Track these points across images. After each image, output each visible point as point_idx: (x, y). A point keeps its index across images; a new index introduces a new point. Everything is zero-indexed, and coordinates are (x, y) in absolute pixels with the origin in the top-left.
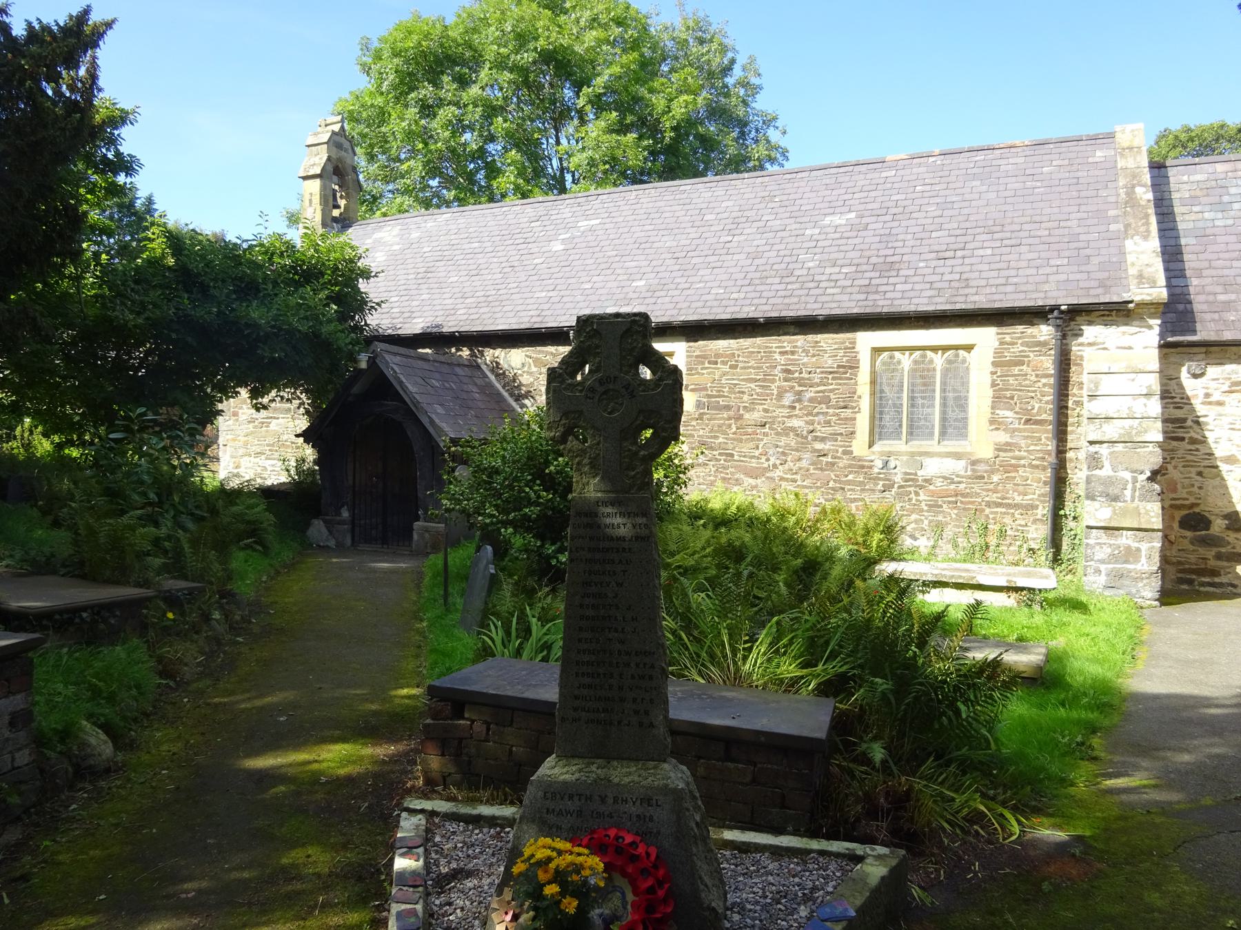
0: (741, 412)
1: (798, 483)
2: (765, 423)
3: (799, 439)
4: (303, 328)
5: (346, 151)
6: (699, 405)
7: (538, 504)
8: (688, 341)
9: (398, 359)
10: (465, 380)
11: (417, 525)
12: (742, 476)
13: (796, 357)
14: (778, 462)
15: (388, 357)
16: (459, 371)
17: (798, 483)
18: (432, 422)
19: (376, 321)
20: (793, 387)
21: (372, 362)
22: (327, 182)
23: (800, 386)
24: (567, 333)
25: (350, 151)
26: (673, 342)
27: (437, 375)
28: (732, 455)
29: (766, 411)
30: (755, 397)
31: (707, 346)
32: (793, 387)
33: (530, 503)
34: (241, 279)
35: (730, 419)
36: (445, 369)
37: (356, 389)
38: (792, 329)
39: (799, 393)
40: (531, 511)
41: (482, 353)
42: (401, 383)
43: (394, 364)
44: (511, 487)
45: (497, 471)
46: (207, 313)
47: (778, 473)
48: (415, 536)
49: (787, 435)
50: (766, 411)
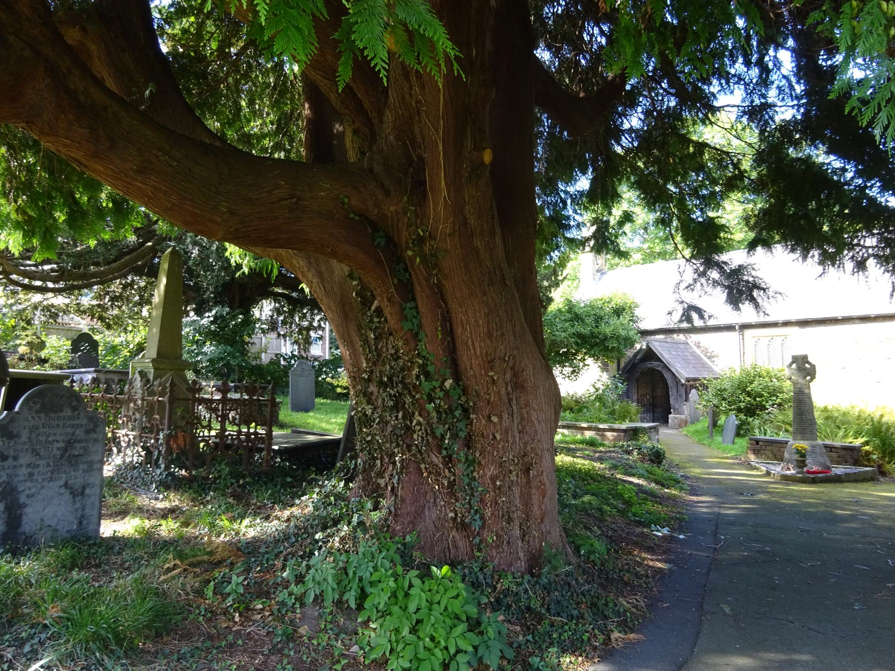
4: (623, 333)
7: (744, 402)
9: (657, 343)
10: (684, 350)
11: (670, 416)
15: (654, 343)
16: (680, 346)
18: (677, 371)
19: (646, 325)
21: (648, 345)
24: (735, 327)
27: (673, 349)
33: (740, 402)
34: (595, 315)
36: (675, 346)
37: (638, 357)
38: (857, 321)
40: (742, 405)
41: (690, 337)
42: (661, 354)
43: (658, 344)
44: (732, 396)
45: (725, 389)
46: (586, 331)
48: (670, 421)
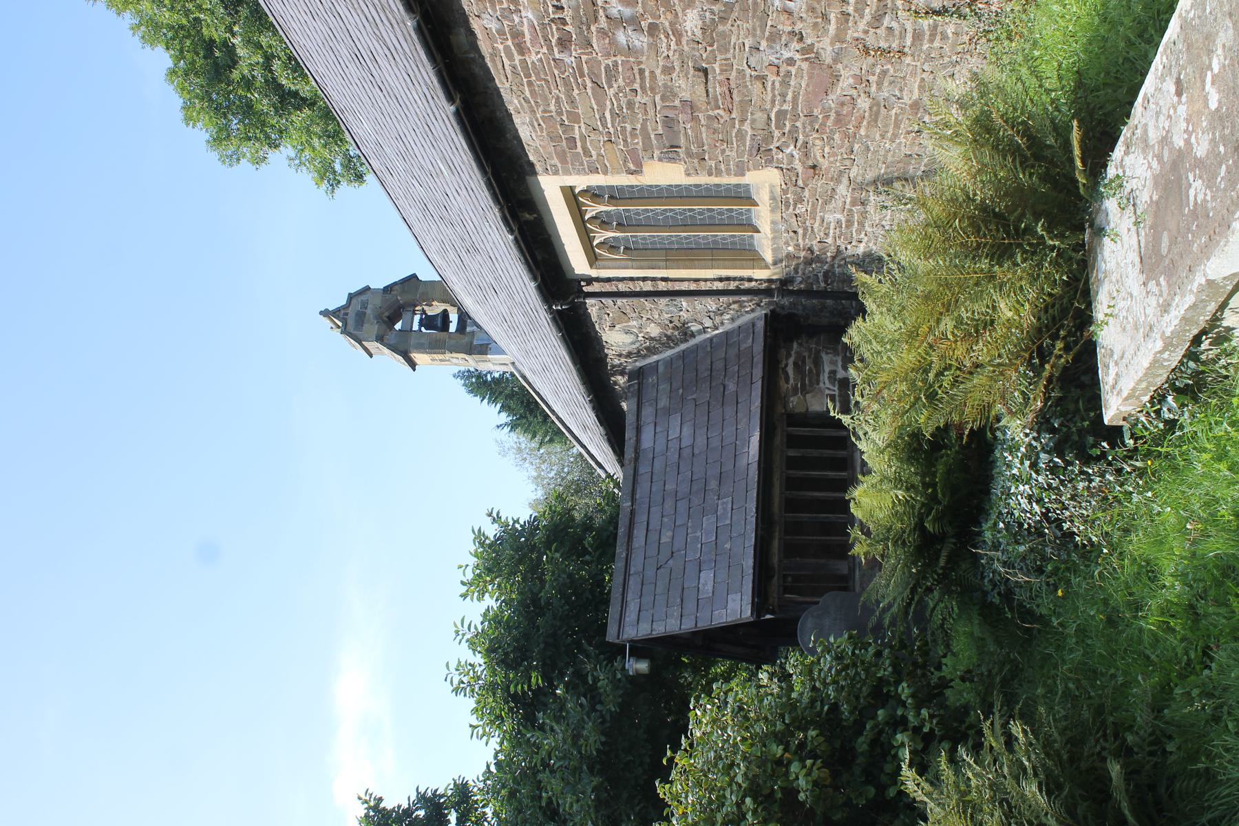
0: (677, 103)
1: (851, 9)
2: (697, 69)
3: (734, 15)
5: (364, 305)
6: (671, 152)
8: (535, 173)
12: (832, 96)
13: (526, 29)
14: (795, 45)
17: (851, 9)
20: (601, 31)
22: (413, 340)
23: (596, 19)
25: (363, 298)
26: (542, 191)
28: (781, 115)
29: (668, 70)
30: (637, 86)
31: (536, 150)
32: (601, 31)
35: (695, 119)
38: (460, 38)
39: (617, 22)
47: (826, 48)
49: (724, 35)
50: (668, 70)
